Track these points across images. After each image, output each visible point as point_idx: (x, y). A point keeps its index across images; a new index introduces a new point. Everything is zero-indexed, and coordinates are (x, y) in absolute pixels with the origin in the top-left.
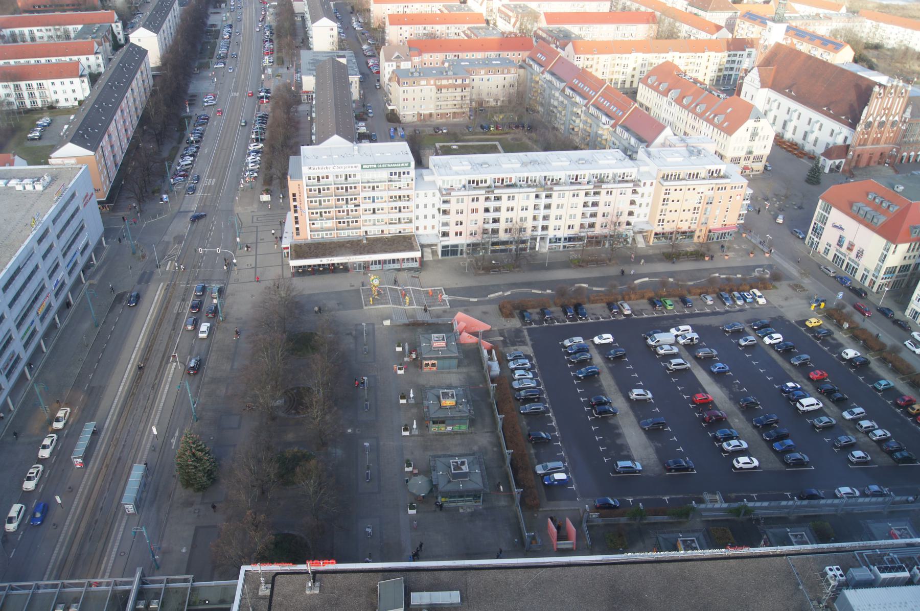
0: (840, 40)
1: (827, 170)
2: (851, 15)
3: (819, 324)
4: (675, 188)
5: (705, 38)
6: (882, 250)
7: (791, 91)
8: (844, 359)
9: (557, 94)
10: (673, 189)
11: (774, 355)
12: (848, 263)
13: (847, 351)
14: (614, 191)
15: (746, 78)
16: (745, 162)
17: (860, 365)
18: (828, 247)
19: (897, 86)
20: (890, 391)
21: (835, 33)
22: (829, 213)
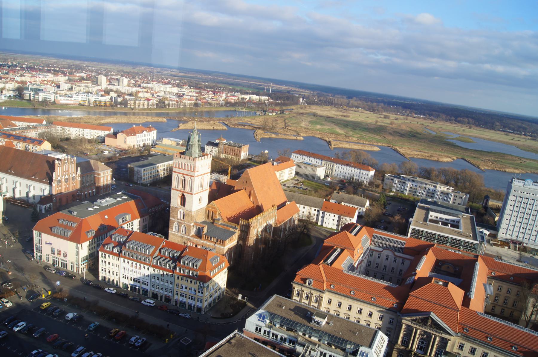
1: (44, 212)
2: (48, 125)
3: (48, 305)
6: (75, 250)
7: (11, 171)
8: (68, 321)
11: (22, 336)
12: (61, 262)
13: (67, 315)
17: (77, 320)
18: (48, 257)
19: (67, 159)
20: (98, 328)
21: (41, 135)
22: (41, 237)
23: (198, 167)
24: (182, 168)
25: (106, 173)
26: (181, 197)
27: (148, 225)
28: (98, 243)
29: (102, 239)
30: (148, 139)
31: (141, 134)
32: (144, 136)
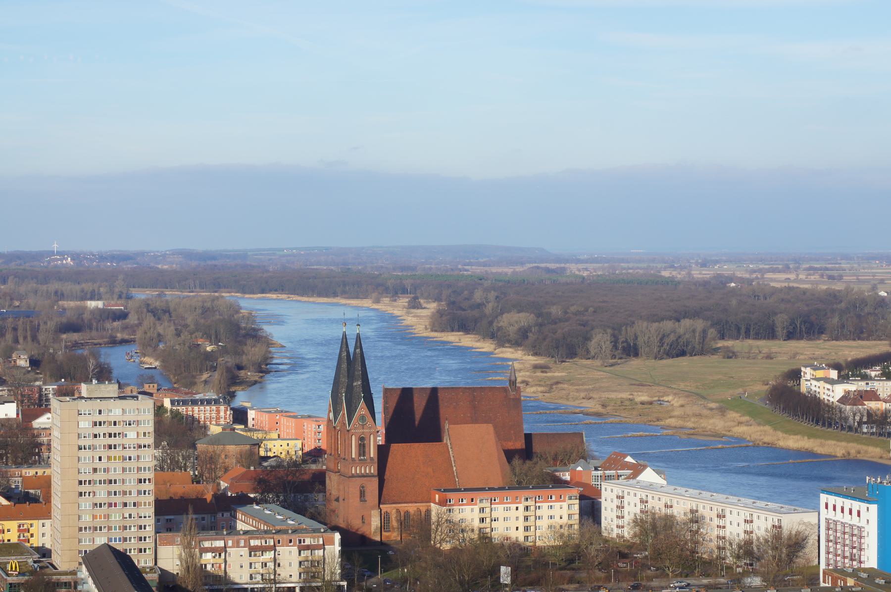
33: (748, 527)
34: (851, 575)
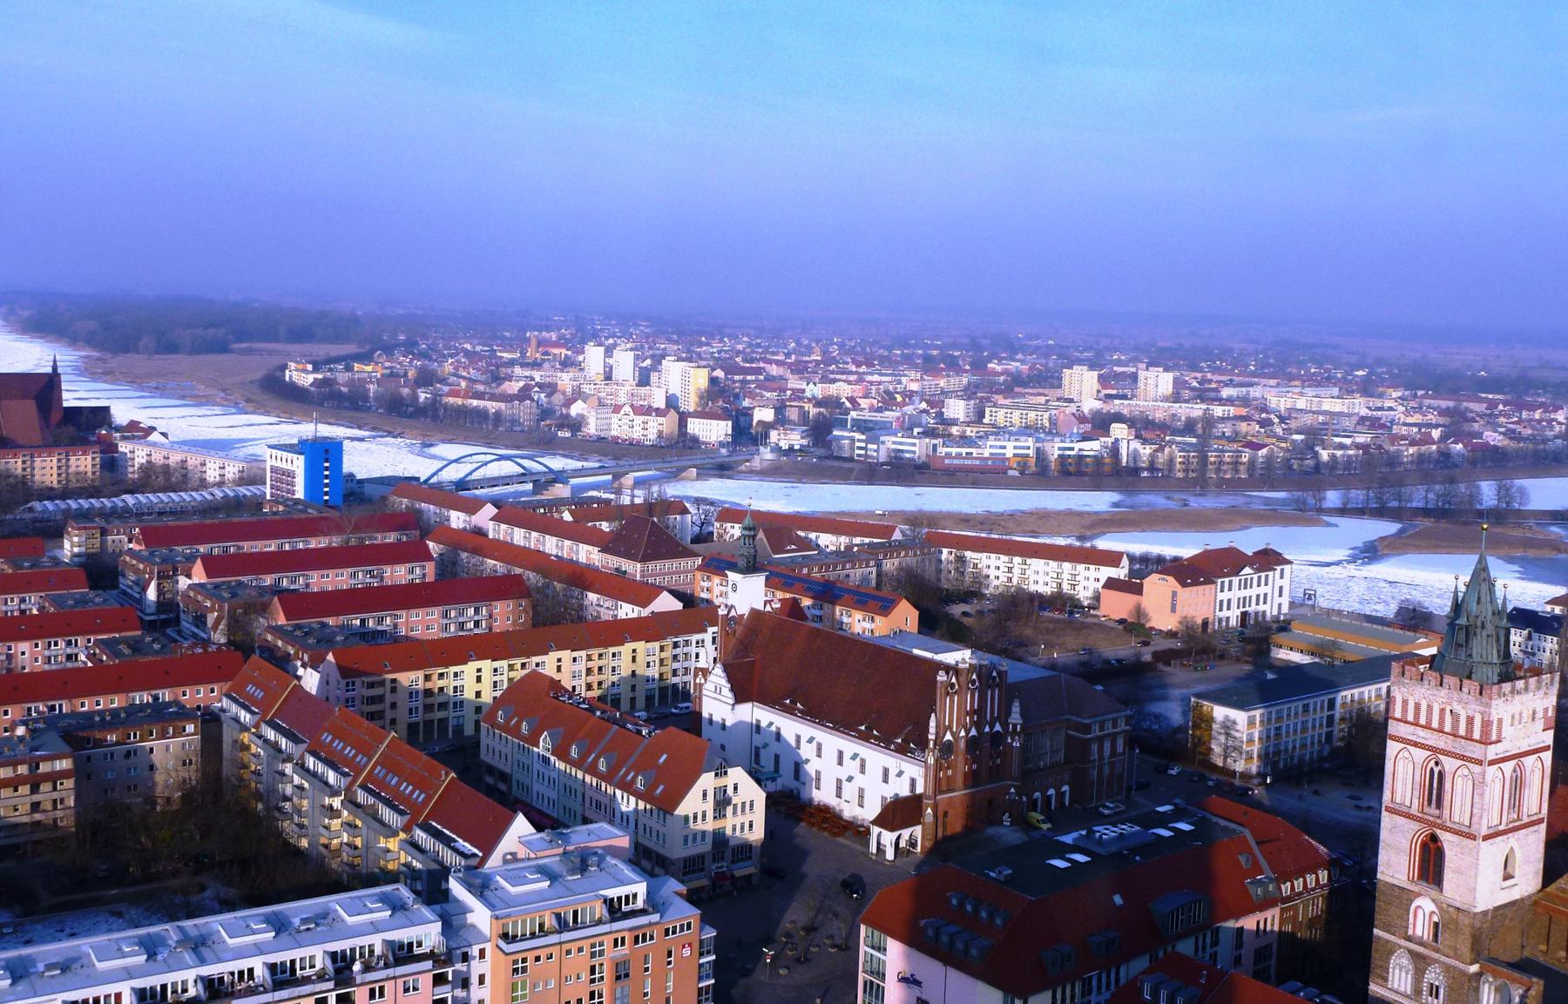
0: (886, 591)
1: (890, 855)
4: (537, 953)
5: (631, 616)
9: (288, 768)
10: (530, 956)
14: (389, 986)
15: (706, 686)
16: (714, 867)
23: (1500, 721)
24: (1428, 727)
25: (1110, 726)
26: (1424, 845)
27: (1275, 947)
28: (1087, 999)
29: (1099, 988)
30: (1258, 596)
31: (1235, 580)
32: (1246, 585)
33: (222, 472)
34: (281, 503)
